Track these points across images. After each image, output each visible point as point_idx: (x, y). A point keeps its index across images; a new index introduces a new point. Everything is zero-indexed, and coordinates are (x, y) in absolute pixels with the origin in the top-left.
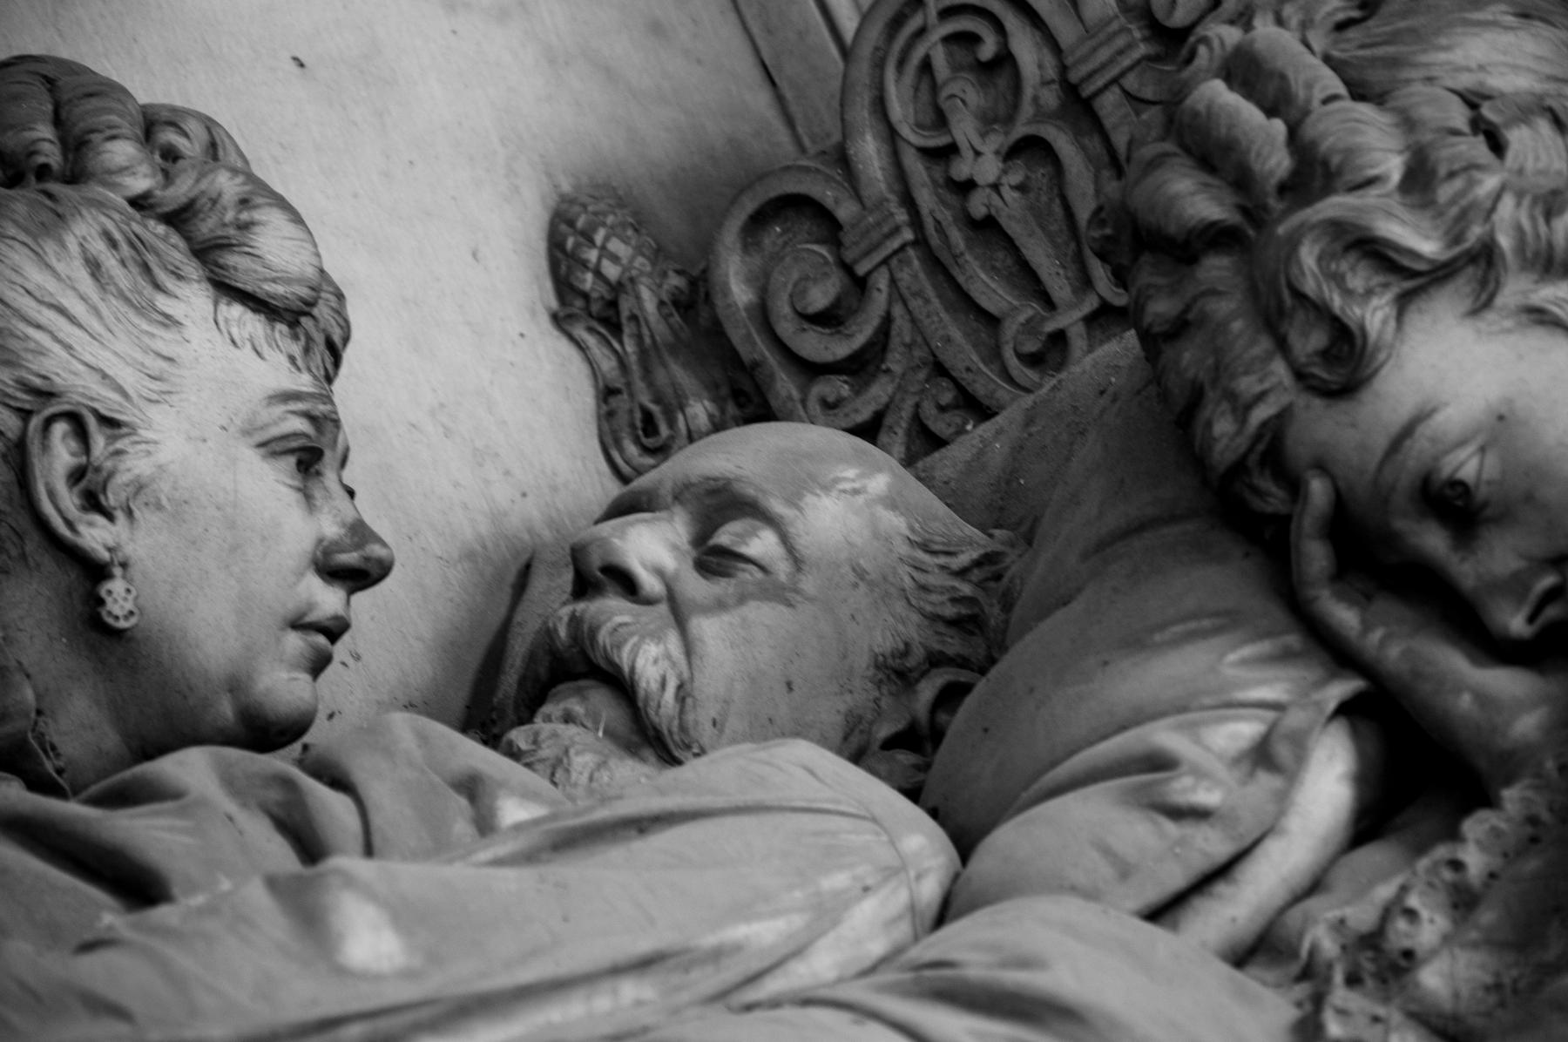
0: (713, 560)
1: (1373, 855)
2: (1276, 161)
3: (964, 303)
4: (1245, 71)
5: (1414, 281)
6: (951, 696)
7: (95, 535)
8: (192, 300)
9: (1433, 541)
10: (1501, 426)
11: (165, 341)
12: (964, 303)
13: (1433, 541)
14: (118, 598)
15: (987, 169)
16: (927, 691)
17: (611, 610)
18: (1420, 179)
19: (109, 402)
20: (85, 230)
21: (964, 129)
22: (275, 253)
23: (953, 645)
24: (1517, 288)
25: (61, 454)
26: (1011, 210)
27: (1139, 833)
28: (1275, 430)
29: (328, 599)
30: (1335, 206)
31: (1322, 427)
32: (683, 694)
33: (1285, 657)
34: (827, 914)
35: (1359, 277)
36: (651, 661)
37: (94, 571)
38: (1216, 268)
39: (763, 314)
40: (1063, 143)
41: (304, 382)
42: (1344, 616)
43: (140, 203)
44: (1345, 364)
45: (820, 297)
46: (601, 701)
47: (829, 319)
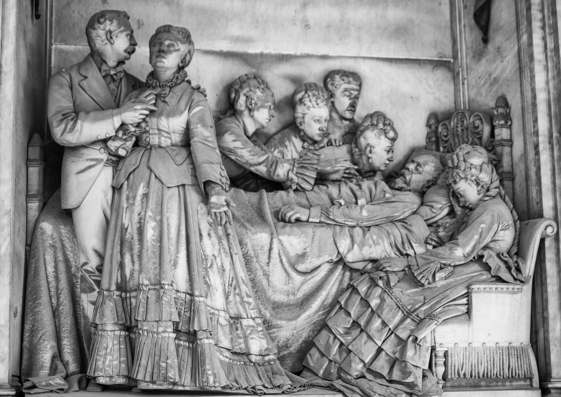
0: (416, 169)
1: (447, 217)
2: (456, 164)
4: (457, 155)
5: (461, 178)
6: (433, 184)
7: (370, 155)
8: (383, 137)
10: (464, 191)
11: (379, 141)
13: (459, 196)
14: (370, 161)
15: (459, 130)
16: (431, 183)
17: (406, 172)
18: (464, 170)
19: (373, 145)
20: (376, 131)
21: (459, 126)
23: (434, 180)
24: (468, 181)
25: (368, 149)
27: (429, 212)
28: (450, 184)
29: (388, 162)
30: (458, 170)
31: (453, 185)
32: (410, 180)
33: (447, 200)
34: (404, 213)
35: (458, 176)
36: (408, 177)
37: (369, 158)
38: (451, 170)
39: (441, 133)
40: (465, 131)
41: (390, 145)
42: (452, 199)
43: (381, 129)
44: (455, 182)
45: (445, 134)
46: (404, 179)
47: (446, 136)
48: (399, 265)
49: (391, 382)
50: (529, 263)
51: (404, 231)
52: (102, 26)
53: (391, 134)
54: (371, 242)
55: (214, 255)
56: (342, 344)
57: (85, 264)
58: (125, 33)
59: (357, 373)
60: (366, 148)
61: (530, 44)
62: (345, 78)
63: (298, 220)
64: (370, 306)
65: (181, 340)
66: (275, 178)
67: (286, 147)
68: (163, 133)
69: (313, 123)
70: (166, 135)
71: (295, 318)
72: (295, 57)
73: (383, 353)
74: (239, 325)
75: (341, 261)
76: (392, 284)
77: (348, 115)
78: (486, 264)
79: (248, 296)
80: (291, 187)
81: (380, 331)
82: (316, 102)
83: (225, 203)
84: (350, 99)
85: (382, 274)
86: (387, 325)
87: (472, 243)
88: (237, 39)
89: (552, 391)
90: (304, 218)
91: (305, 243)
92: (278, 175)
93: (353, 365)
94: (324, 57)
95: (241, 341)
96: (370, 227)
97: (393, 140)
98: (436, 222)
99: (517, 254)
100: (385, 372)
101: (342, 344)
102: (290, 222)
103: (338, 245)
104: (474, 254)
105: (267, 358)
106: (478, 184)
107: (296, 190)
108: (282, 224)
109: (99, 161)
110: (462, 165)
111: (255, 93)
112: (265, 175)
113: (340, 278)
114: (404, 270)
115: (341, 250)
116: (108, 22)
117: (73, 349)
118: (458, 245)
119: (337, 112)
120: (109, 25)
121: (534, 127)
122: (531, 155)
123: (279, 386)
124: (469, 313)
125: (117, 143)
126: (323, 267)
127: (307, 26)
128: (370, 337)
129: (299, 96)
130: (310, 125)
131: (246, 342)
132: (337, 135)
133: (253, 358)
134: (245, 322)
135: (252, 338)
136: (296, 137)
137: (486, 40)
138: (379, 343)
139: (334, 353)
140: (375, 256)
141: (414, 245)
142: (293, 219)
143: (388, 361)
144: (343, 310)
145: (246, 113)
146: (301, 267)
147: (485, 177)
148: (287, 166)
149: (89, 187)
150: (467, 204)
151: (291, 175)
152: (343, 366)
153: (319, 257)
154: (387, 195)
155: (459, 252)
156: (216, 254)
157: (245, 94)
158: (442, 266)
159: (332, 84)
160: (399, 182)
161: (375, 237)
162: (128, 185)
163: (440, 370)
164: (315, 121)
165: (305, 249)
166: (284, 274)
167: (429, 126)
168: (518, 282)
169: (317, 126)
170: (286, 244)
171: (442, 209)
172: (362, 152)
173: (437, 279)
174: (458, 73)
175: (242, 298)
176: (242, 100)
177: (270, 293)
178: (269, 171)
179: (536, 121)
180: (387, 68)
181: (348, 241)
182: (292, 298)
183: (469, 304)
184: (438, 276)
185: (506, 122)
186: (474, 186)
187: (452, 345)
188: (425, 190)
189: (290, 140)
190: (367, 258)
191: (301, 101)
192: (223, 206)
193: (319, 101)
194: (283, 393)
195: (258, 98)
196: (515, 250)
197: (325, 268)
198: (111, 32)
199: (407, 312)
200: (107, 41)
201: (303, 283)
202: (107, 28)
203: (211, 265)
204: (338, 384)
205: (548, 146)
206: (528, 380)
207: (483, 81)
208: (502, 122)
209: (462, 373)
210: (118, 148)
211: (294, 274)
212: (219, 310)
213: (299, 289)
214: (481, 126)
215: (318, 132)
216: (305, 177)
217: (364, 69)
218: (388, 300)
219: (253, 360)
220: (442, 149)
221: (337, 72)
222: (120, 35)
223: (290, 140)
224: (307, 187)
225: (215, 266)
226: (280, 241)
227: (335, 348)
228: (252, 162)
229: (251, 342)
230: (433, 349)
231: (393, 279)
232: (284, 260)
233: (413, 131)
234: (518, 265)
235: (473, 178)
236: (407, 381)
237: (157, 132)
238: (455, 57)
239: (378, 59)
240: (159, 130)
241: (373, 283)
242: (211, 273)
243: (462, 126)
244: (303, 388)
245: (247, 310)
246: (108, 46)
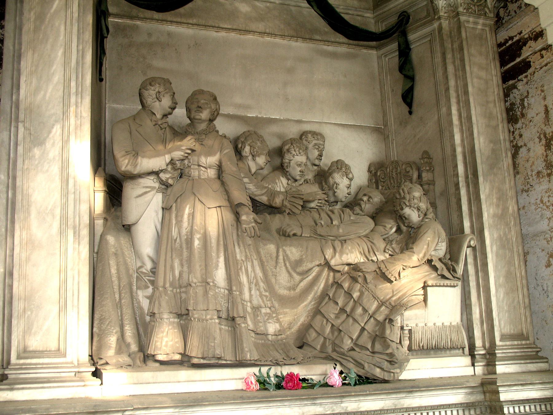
0: (368, 200)
1: (395, 234)
3: (390, 181)
4: (403, 190)
5: (407, 206)
7: (336, 190)
8: (345, 178)
9: (404, 219)
10: (409, 215)
12: (390, 181)
13: (404, 219)
14: (336, 194)
17: (362, 202)
18: (409, 201)
20: (340, 173)
21: (394, 171)
22: (350, 176)
24: (412, 208)
25: (335, 186)
26: (395, 177)
27: (383, 230)
29: (347, 195)
30: (404, 201)
31: (400, 211)
36: (363, 206)
39: (379, 176)
44: (402, 209)
48: (372, 267)
49: (373, 353)
50: (460, 265)
51: (369, 243)
52: (153, 88)
53: (350, 176)
54: (347, 251)
55: (242, 260)
56: (333, 325)
57: (141, 267)
58: (169, 94)
59: (348, 347)
60: (333, 185)
61: (450, 114)
62: (315, 136)
63: (294, 235)
64: (352, 297)
65: (222, 325)
67: (276, 183)
68: (202, 168)
69: (297, 167)
70: (204, 169)
72: (280, 120)
73: (366, 332)
74: (259, 313)
75: (327, 264)
76: (368, 281)
77: (317, 162)
78: (435, 266)
79: (266, 291)
80: (285, 211)
81: (361, 315)
82: (299, 151)
83: (253, 220)
84: (318, 151)
85: (360, 274)
86: (367, 311)
87: (423, 251)
88: (239, 106)
89: (477, 356)
90: (299, 233)
91: (301, 251)
92: (276, 203)
93: (344, 341)
94: (299, 122)
96: (345, 240)
97: (351, 180)
98: (388, 237)
99: (449, 259)
100: (369, 347)
101: (333, 325)
102: (289, 236)
103: (325, 253)
104: (426, 259)
105: (279, 337)
106: (418, 209)
107: (289, 214)
108: (283, 238)
109: (153, 188)
110: (407, 196)
111: (256, 144)
112: (267, 203)
113: (326, 277)
114: (376, 271)
115: (327, 257)
116: (158, 85)
117: (134, 333)
118: (414, 253)
119: (310, 160)
120: (157, 88)
121: (454, 171)
122: (452, 190)
123: (294, 359)
124: (425, 300)
125: (168, 176)
126: (314, 269)
127: (287, 99)
128: (355, 320)
129: (287, 147)
130: (294, 168)
131: (265, 326)
132: (310, 176)
133: (270, 337)
134: (263, 311)
135: (269, 323)
136: (283, 177)
137: (410, 113)
138: (363, 325)
139: (328, 332)
140: (350, 261)
141: (376, 253)
142: (291, 233)
143: (370, 337)
144: (331, 301)
145: (250, 158)
146: (300, 269)
147: (423, 206)
148: (281, 197)
149: (145, 206)
150: (411, 224)
151: (286, 203)
152: (336, 342)
153: (312, 262)
154: (352, 218)
155: (415, 258)
156: (244, 259)
157: (249, 145)
158: (404, 267)
159: (306, 140)
160: (357, 209)
161: (350, 248)
162: (176, 207)
163: (406, 343)
164: (297, 165)
165: (302, 256)
166: (287, 275)
167: (369, 171)
168: (456, 279)
169: (299, 169)
170: (288, 252)
171: (391, 228)
172: (331, 188)
173: (401, 277)
174: (388, 136)
175: (260, 293)
176: (247, 149)
177: (277, 287)
178: (269, 200)
179: (456, 166)
181: (331, 250)
182: (292, 292)
183: (425, 295)
184: (402, 275)
185: (430, 169)
186: (416, 211)
187: (415, 326)
188: (374, 215)
189: (279, 179)
190: (345, 262)
191: (288, 151)
192: (252, 223)
193: (301, 151)
194: (298, 363)
196: (448, 256)
197: (316, 269)
198: (159, 92)
199: (381, 301)
200: (156, 99)
202: (157, 90)
204: (334, 355)
205: (465, 184)
206: (461, 349)
207: (408, 141)
208: (428, 168)
209: (421, 345)
210: (168, 179)
211: (295, 275)
212: (246, 302)
213: (298, 285)
214: (411, 171)
215: (299, 173)
216: (295, 204)
217: (326, 131)
218: (366, 293)
219: (270, 339)
220: (380, 187)
221: (310, 132)
222: (166, 95)
223: (279, 179)
224: (297, 211)
225: (243, 268)
226: (284, 251)
227: (328, 329)
228: (257, 193)
229: (268, 325)
230: (402, 328)
231: (369, 278)
232: (288, 264)
233: (360, 175)
234: (453, 267)
235: (416, 206)
236: (387, 352)
237: (197, 167)
238: (386, 125)
239: (335, 124)
240: (199, 166)
241: (354, 280)
243: (396, 171)
244: (309, 359)
245: (265, 301)
246: (157, 103)
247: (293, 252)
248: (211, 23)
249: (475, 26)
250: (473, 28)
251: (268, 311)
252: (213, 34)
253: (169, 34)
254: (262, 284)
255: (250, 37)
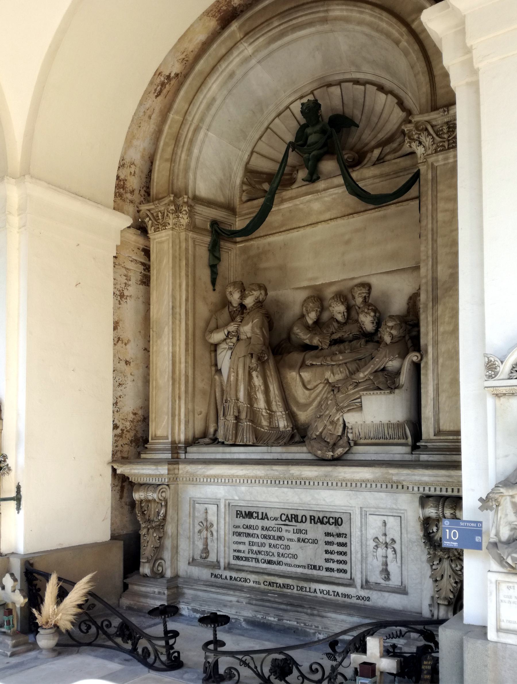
66: (313, 344)
67: (330, 328)
71: (306, 411)
79: (279, 402)
88: (311, 279)
95: (276, 422)
111: (309, 305)
126: (319, 386)
127: (344, 265)
153: (315, 381)
156: (261, 384)
180: (385, 277)
195: (310, 307)
197: (321, 386)
201: (311, 394)
203: (258, 390)
229: (280, 422)
242: (257, 393)
247: (306, 375)
248: (294, 226)
249: (446, 162)
250: (444, 165)
251: (280, 414)
252: (295, 234)
253: (269, 244)
254: (277, 398)
255: (320, 226)
